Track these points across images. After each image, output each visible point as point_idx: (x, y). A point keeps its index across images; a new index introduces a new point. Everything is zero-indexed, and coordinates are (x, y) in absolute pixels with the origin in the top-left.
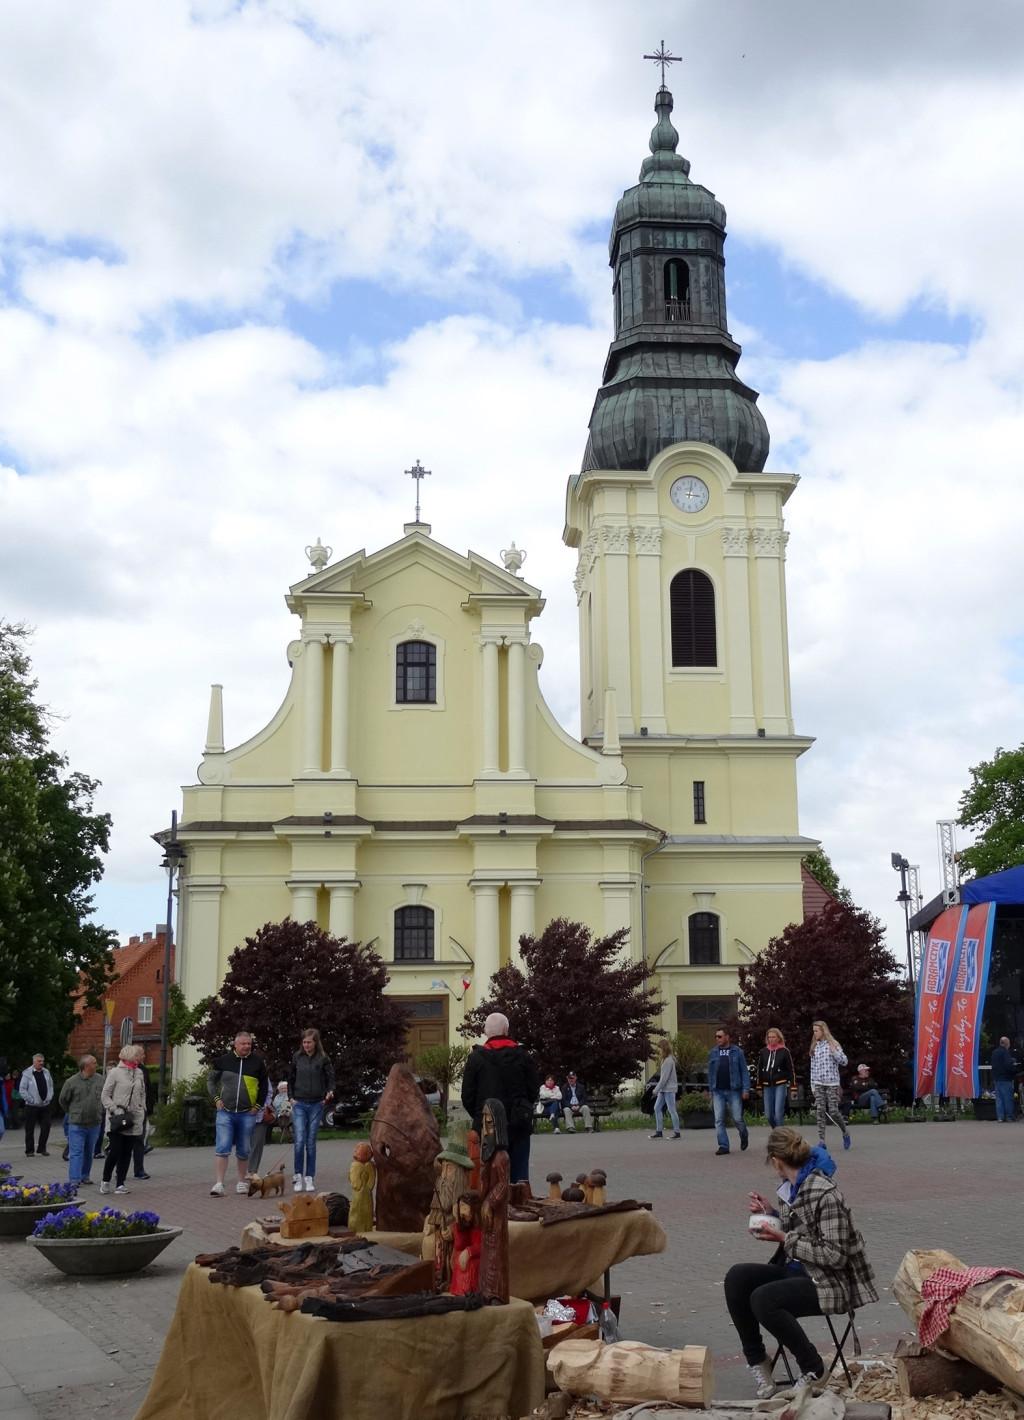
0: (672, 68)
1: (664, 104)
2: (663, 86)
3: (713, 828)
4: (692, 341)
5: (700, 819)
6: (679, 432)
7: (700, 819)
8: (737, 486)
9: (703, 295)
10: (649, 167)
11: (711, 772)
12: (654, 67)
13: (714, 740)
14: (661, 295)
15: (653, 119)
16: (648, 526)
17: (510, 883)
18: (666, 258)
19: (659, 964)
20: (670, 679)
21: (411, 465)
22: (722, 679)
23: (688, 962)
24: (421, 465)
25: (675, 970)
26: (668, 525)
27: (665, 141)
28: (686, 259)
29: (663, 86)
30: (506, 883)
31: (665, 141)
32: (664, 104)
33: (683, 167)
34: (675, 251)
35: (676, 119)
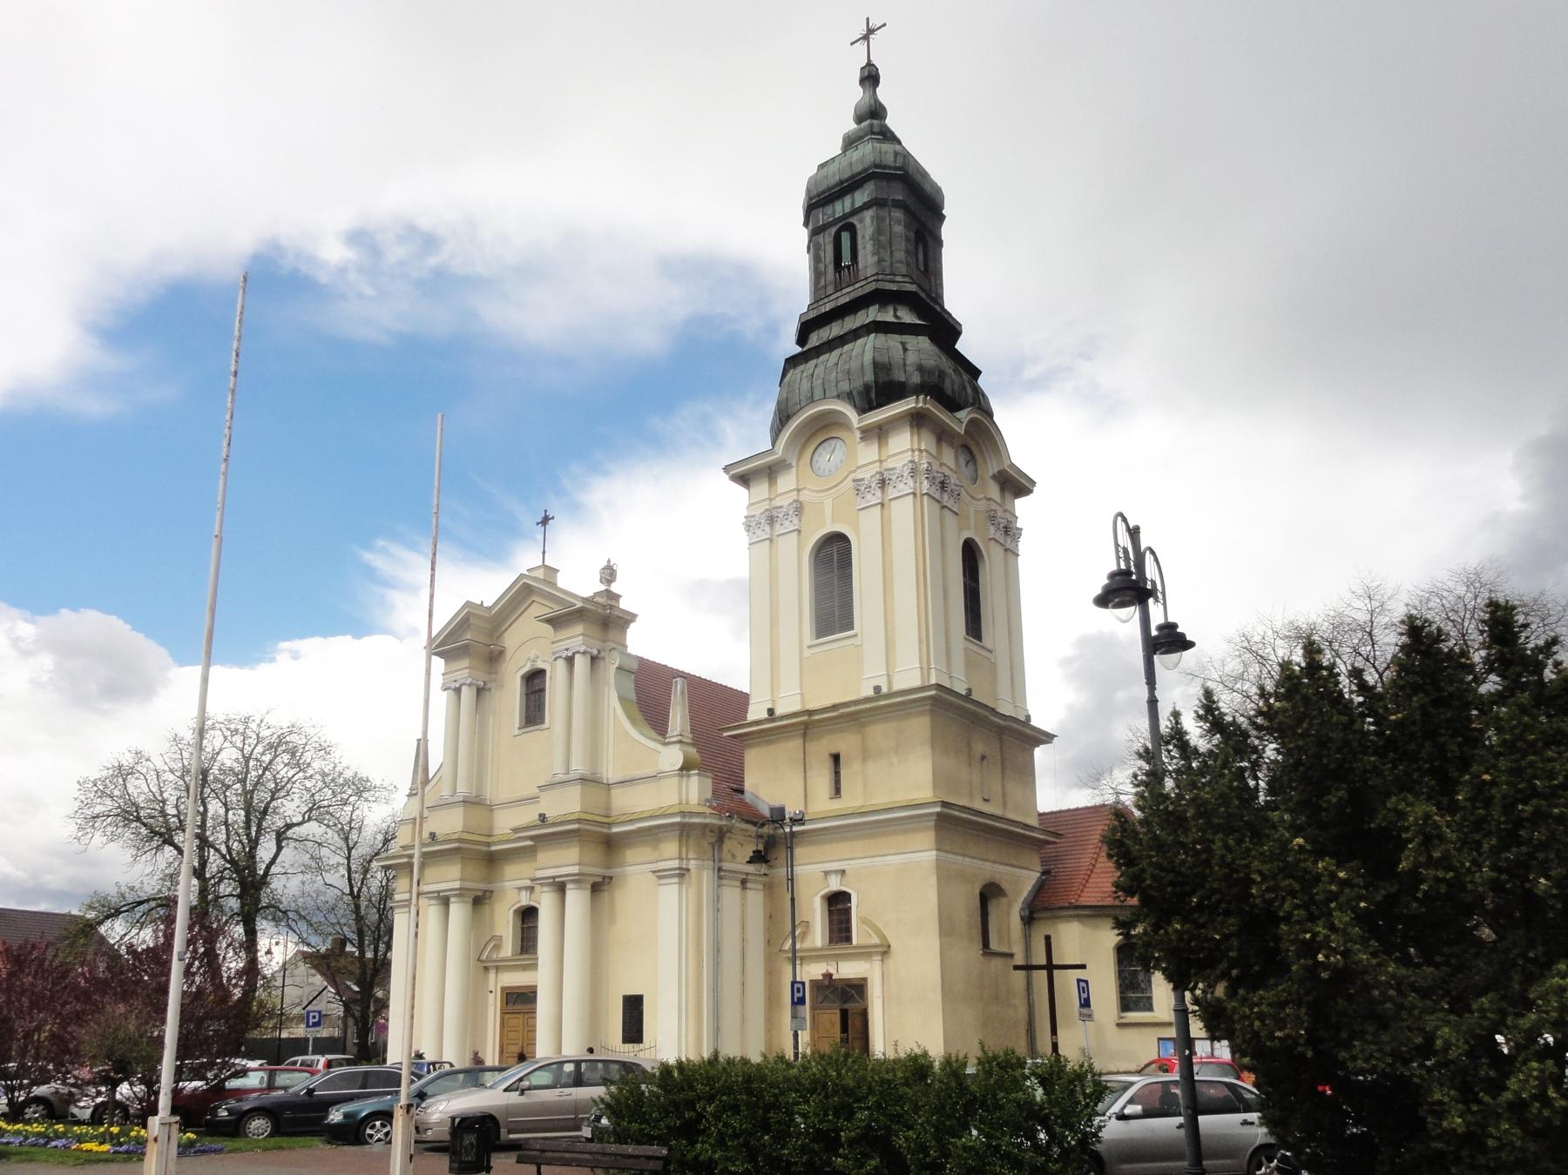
1: (870, 78)
2: (869, 64)
3: (852, 799)
6: (818, 394)
7: (837, 791)
8: (869, 433)
9: (869, 247)
10: (850, 142)
11: (844, 743)
12: (862, 46)
13: (835, 707)
14: (831, 268)
15: (857, 94)
16: (785, 503)
18: (833, 230)
20: (807, 653)
22: (856, 641)
26: (805, 496)
28: (854, 220)
32: (870, 78)
34: (845, 216)
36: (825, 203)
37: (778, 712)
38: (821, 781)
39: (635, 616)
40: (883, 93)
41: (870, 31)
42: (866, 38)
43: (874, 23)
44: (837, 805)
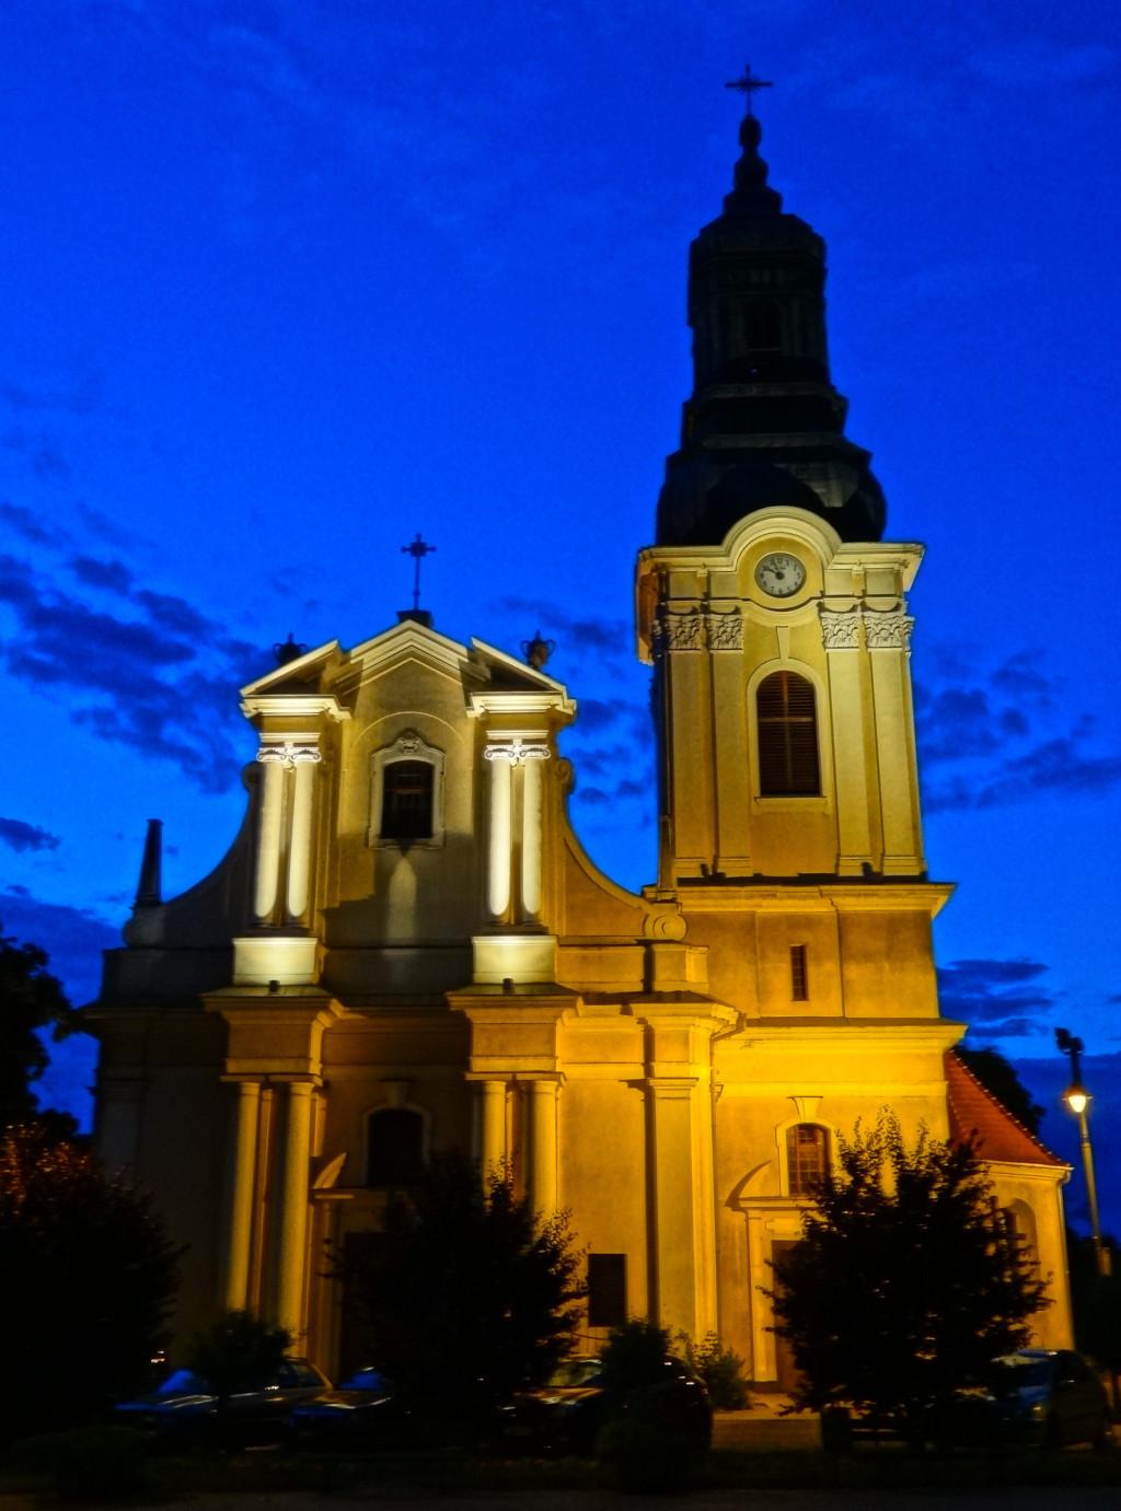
0: (760, 98)
1: (750, 132)
4: (781, 393)
5: (800, 991)
7: (800, 991)
12: (739, 98)
15: (736, 152)
17: (520, 1077)
19: (744, 1194)
21: (409, 541)
23: (785, 1191)
24: (423, 540)
25: (769, 1204)
27: (751, 171)
30: (514, 1077)
31: (751, 171)
32: (750, 132)
33: (775, 199)
35: (763, 150)
36: (712, 264)
38: (782, 978)
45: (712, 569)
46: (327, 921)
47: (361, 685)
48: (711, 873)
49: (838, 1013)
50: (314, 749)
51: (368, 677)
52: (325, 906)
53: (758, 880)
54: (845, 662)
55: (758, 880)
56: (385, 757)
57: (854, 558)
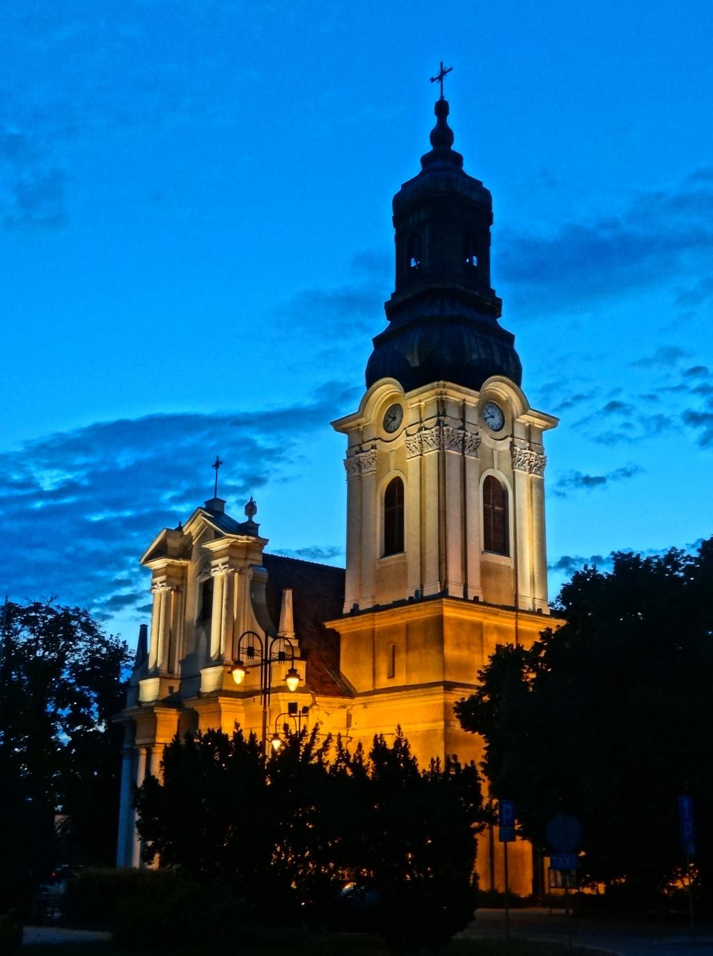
1: (442, 109)
5: (392, 675)
7: (392, 675)
27: (442, 136)
29: (442, 97)
31: (442, 136)
32: (442, 109)
37: (361, 608)
39: (267, 540)
40: (451, 121)
41: (443, 73)
42: (440, 78)
43: (447, 66)
44: (391, 684)
45: (365, 424)
46: (181, 666)
47: (193, 543)
48: (419, 596)
49: (371, 689)
50: (164, 584)
51: (195, 538)
52: (181, 658)
53: (377, 609)
54: (412, 463)
55: (377, 609)
56: (200, 579)
57: (416, 399)
